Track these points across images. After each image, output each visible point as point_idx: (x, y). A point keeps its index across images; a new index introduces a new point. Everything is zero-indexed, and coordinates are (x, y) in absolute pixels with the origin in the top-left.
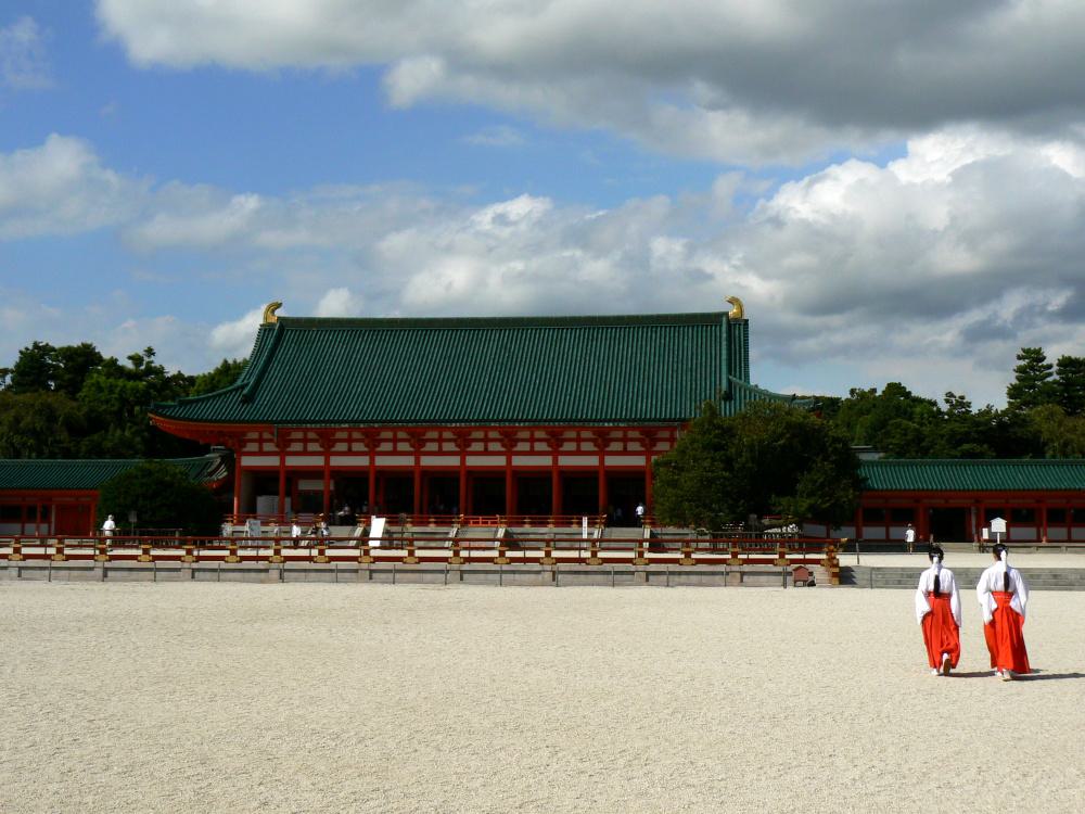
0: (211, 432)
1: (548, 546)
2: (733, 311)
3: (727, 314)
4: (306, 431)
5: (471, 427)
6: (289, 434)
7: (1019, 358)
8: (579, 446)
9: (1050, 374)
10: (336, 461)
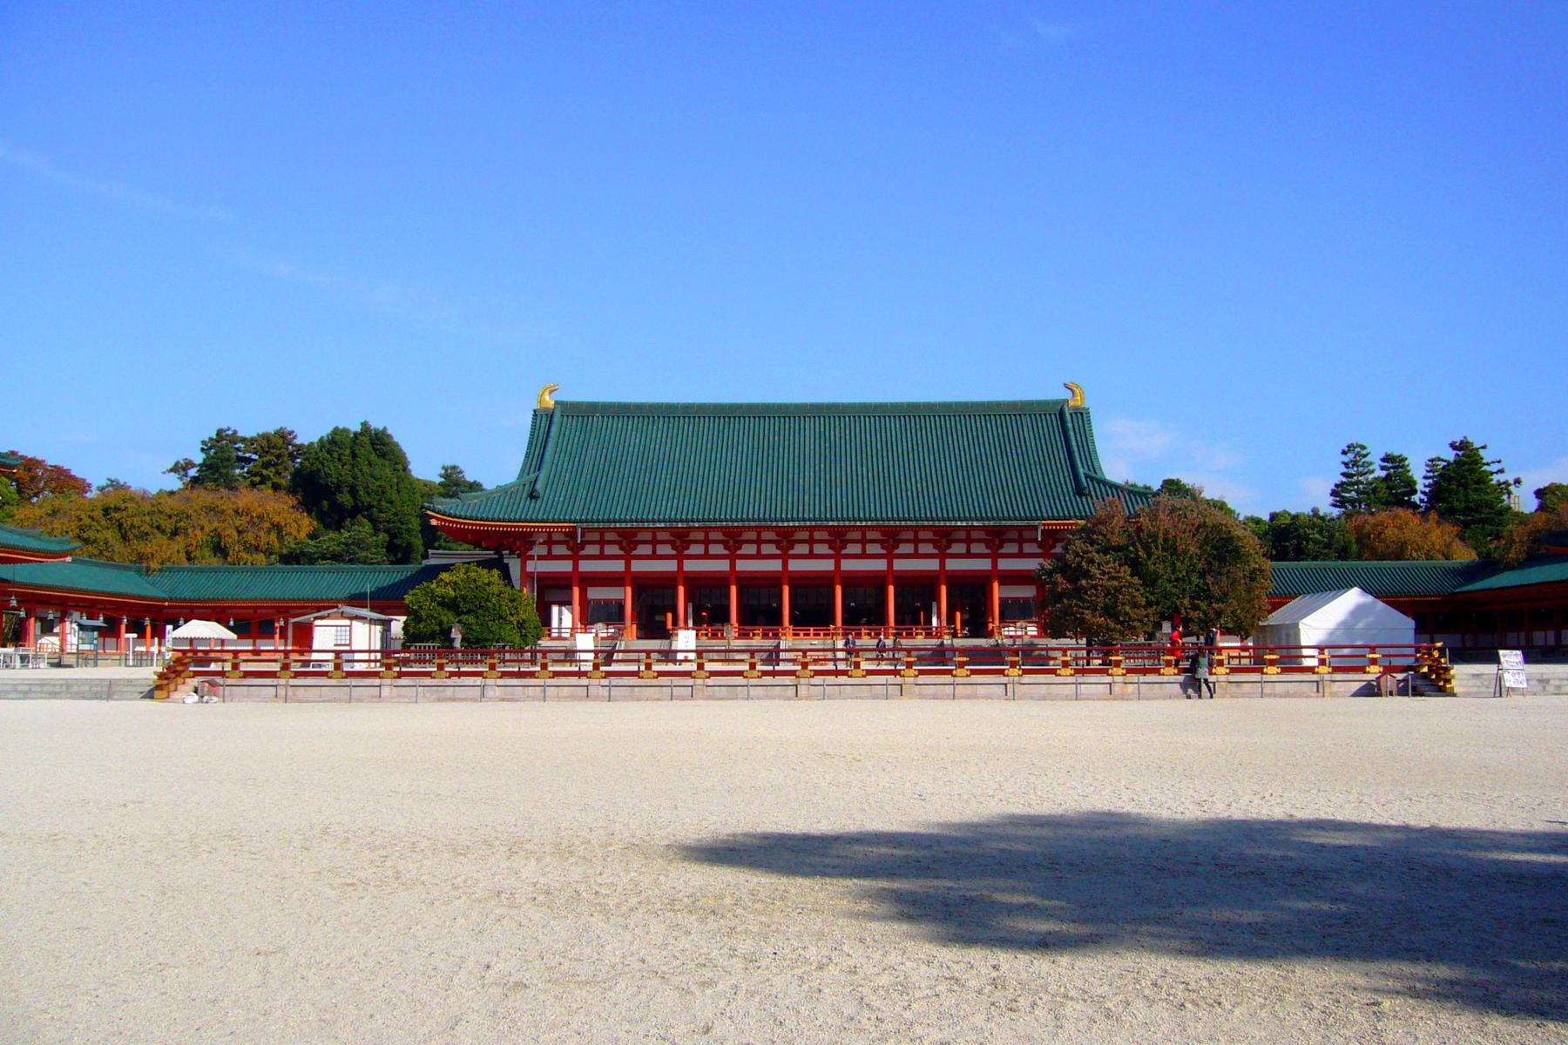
4: (654, 531)
7: (1344, 453)
9: (1372, 472)
10: (638, 566)
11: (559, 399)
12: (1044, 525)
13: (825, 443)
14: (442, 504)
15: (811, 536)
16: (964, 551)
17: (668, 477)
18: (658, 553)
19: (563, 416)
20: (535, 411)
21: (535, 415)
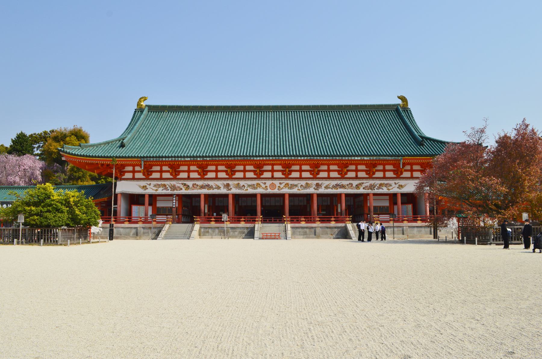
0: (102, 165)
2: (399, 102)
3: (399, 105)
11: (147, 104)
12: (404, 159)
13: (279, 122)
14: (69, 148)
17: (197, 137)
19: (149, 112)
20: (135, 110)
21: (135, 112)
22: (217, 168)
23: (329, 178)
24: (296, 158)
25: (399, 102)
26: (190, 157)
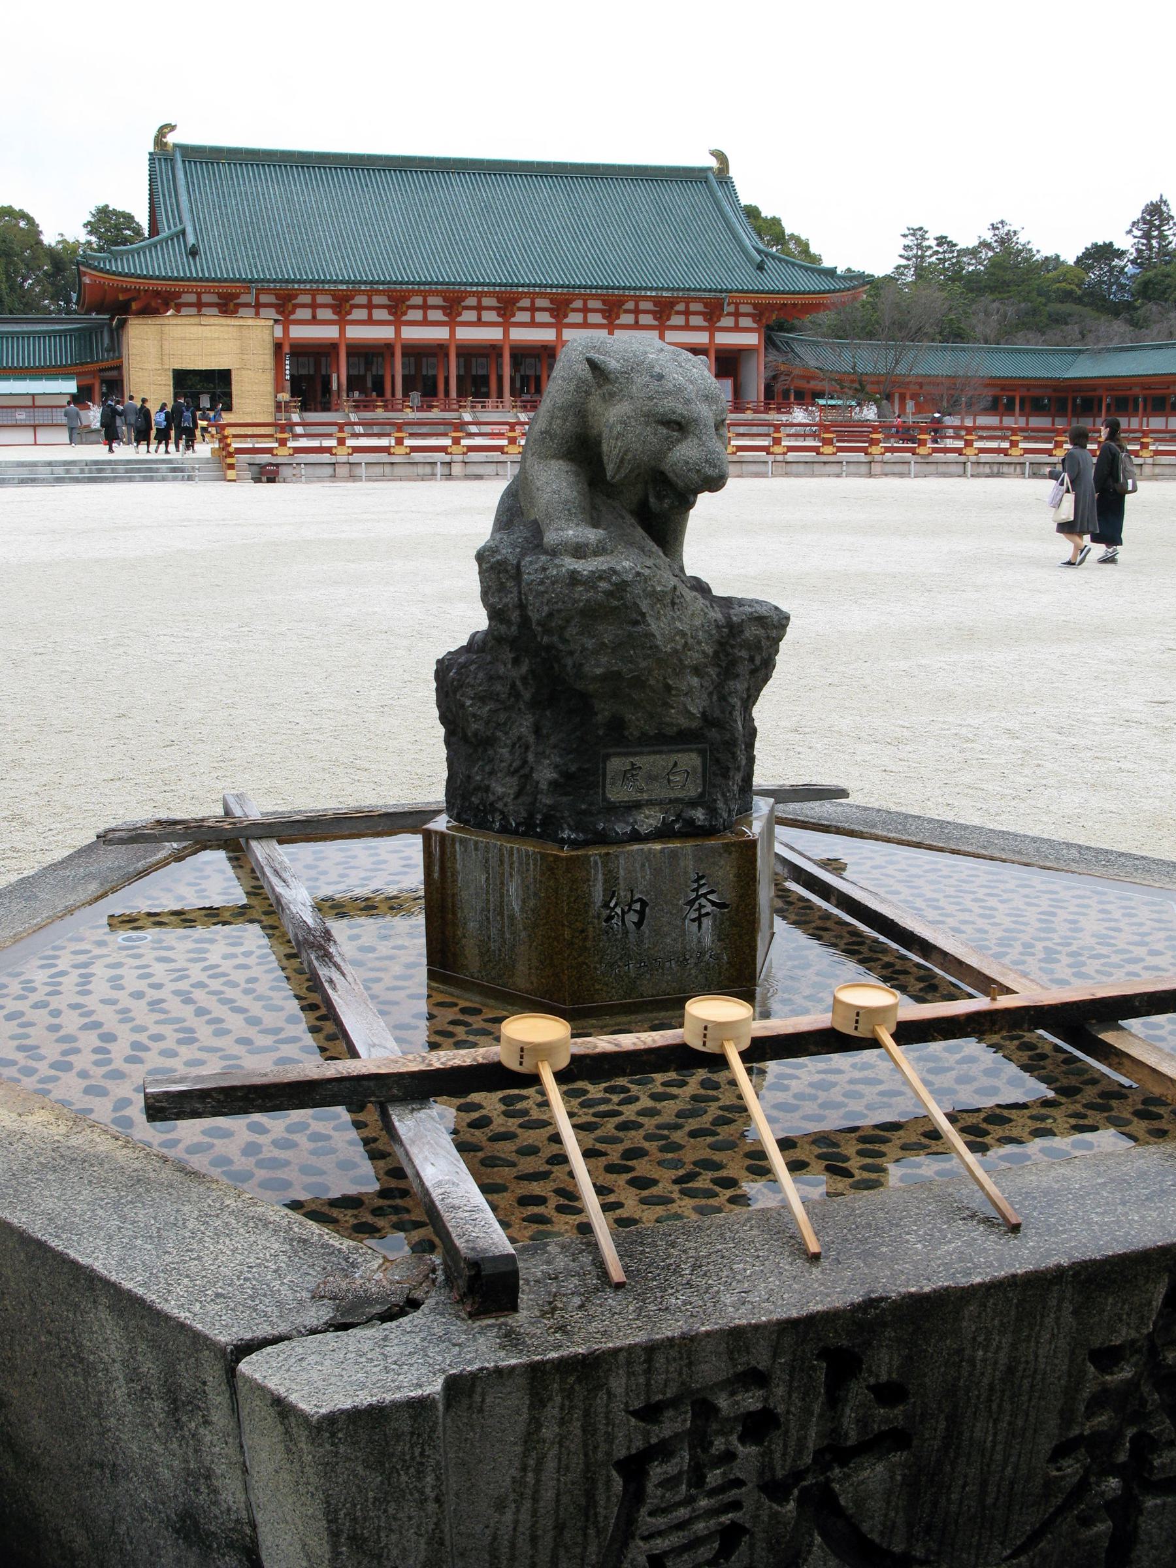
1: (341, 431)
2: (713, 163)
3: (710, 169)
5: (573, 294)
6: (296, 296)
7: (905, 236)
8: (585, 318)
15: (370, 300)
16: (581, 321)
18: (741, 325)
20: (150, 154)
22: (370, 300)
23: (585, 325)
24: (543, 290)
25: (713, 163)
26: (347, 282)
